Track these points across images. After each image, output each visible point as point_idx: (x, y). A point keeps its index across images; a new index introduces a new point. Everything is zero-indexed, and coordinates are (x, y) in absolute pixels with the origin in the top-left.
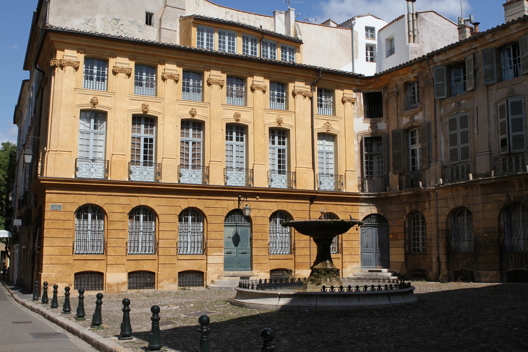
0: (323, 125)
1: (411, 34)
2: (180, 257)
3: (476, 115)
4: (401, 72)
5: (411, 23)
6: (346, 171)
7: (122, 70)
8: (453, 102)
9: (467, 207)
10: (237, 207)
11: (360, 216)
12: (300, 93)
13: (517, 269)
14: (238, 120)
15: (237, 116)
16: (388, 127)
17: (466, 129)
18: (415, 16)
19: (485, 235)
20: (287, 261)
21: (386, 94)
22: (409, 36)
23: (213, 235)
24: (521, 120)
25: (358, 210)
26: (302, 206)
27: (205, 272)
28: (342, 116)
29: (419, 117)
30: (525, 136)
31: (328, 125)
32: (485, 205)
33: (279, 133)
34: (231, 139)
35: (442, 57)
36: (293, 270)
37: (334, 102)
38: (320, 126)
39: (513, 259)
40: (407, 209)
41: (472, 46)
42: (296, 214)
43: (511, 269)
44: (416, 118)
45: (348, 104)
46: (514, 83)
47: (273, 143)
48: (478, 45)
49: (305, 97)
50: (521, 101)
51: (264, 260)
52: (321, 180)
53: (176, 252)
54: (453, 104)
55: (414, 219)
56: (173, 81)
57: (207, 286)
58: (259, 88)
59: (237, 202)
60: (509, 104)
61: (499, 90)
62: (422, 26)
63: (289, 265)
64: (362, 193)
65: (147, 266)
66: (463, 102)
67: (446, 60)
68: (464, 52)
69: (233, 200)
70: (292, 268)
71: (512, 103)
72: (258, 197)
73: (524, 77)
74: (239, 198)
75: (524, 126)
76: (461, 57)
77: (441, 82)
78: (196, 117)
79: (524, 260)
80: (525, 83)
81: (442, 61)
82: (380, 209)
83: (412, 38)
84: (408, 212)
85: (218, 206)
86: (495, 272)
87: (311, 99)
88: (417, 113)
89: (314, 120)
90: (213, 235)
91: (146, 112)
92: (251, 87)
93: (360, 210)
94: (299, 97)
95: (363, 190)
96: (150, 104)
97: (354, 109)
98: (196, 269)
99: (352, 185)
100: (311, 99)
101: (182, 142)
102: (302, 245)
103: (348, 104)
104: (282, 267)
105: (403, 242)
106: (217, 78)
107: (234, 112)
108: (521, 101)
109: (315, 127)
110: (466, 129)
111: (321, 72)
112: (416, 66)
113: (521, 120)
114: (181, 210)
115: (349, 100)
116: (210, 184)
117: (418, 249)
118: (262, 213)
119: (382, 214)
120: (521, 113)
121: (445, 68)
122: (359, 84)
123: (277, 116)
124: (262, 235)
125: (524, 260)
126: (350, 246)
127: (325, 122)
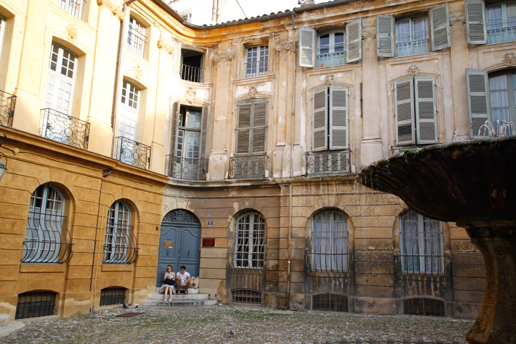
1: (215, 11)
3: (358, 93)
4: (244, 29)
6: (153, 142)
8: (324, 74)
9: (342, 208)
11: (163, 210)
12: (109, 6)
13: (420, 297)
16: (213, 96)
17: (342, 108)
19: (371, 248)
20: (52, 277)
21: (212, 55)
24: (431, 105)
25: (161, 201)
26: (90, 181)
29: (266, 88)
30: (436, 125)
32: (372, 208)
35: (314, 16)
36: (62, 293)
37: (147, 43)
39: (414, 283)
40: (236, 207)
41: (363, 7)
42: (79, 194)
43: (411, 296)
44: (260, 89)
45: (164, 51)
46: (419, 60)
47: (53, 67)
48: (372, 8)
49: (115, 14)
50: (430, 83)
51: (9, 275)
52: (124, 147)
54: (323, 77)
55: (240, 222)
60: (416, 83)
61: (395, 66)
63: (55, 283)
64: (171, 178)
66: (339, 75)
67: (319, 21)
68: (348, 15)
70: (58, 289)
71: (420, 83)
72: (17, 150)
73: (436, 54)
75: (435, 112)
76: (342, 21)
77: (308, 48)
79: (432, 285)
80: (436, 61)
81: (311, 22)
82: (190, 203)
83: (215, 15)
84: (237, 211)
86: (386, 300)
88: (261, 82)
93: (163, 201)
95: (171, 174)
100: (122, 22)
104: (43, 288)
105: (225, 251)
108: (430, 83)
110: (342, 108)
112: (270, 24)
113: (431, 105)
117: (246, 263)
118: (19, 183)
120: (431, 96)
121: (314, 32)
124: (14, 224)
125: (432, 285)
126: (146, 254)
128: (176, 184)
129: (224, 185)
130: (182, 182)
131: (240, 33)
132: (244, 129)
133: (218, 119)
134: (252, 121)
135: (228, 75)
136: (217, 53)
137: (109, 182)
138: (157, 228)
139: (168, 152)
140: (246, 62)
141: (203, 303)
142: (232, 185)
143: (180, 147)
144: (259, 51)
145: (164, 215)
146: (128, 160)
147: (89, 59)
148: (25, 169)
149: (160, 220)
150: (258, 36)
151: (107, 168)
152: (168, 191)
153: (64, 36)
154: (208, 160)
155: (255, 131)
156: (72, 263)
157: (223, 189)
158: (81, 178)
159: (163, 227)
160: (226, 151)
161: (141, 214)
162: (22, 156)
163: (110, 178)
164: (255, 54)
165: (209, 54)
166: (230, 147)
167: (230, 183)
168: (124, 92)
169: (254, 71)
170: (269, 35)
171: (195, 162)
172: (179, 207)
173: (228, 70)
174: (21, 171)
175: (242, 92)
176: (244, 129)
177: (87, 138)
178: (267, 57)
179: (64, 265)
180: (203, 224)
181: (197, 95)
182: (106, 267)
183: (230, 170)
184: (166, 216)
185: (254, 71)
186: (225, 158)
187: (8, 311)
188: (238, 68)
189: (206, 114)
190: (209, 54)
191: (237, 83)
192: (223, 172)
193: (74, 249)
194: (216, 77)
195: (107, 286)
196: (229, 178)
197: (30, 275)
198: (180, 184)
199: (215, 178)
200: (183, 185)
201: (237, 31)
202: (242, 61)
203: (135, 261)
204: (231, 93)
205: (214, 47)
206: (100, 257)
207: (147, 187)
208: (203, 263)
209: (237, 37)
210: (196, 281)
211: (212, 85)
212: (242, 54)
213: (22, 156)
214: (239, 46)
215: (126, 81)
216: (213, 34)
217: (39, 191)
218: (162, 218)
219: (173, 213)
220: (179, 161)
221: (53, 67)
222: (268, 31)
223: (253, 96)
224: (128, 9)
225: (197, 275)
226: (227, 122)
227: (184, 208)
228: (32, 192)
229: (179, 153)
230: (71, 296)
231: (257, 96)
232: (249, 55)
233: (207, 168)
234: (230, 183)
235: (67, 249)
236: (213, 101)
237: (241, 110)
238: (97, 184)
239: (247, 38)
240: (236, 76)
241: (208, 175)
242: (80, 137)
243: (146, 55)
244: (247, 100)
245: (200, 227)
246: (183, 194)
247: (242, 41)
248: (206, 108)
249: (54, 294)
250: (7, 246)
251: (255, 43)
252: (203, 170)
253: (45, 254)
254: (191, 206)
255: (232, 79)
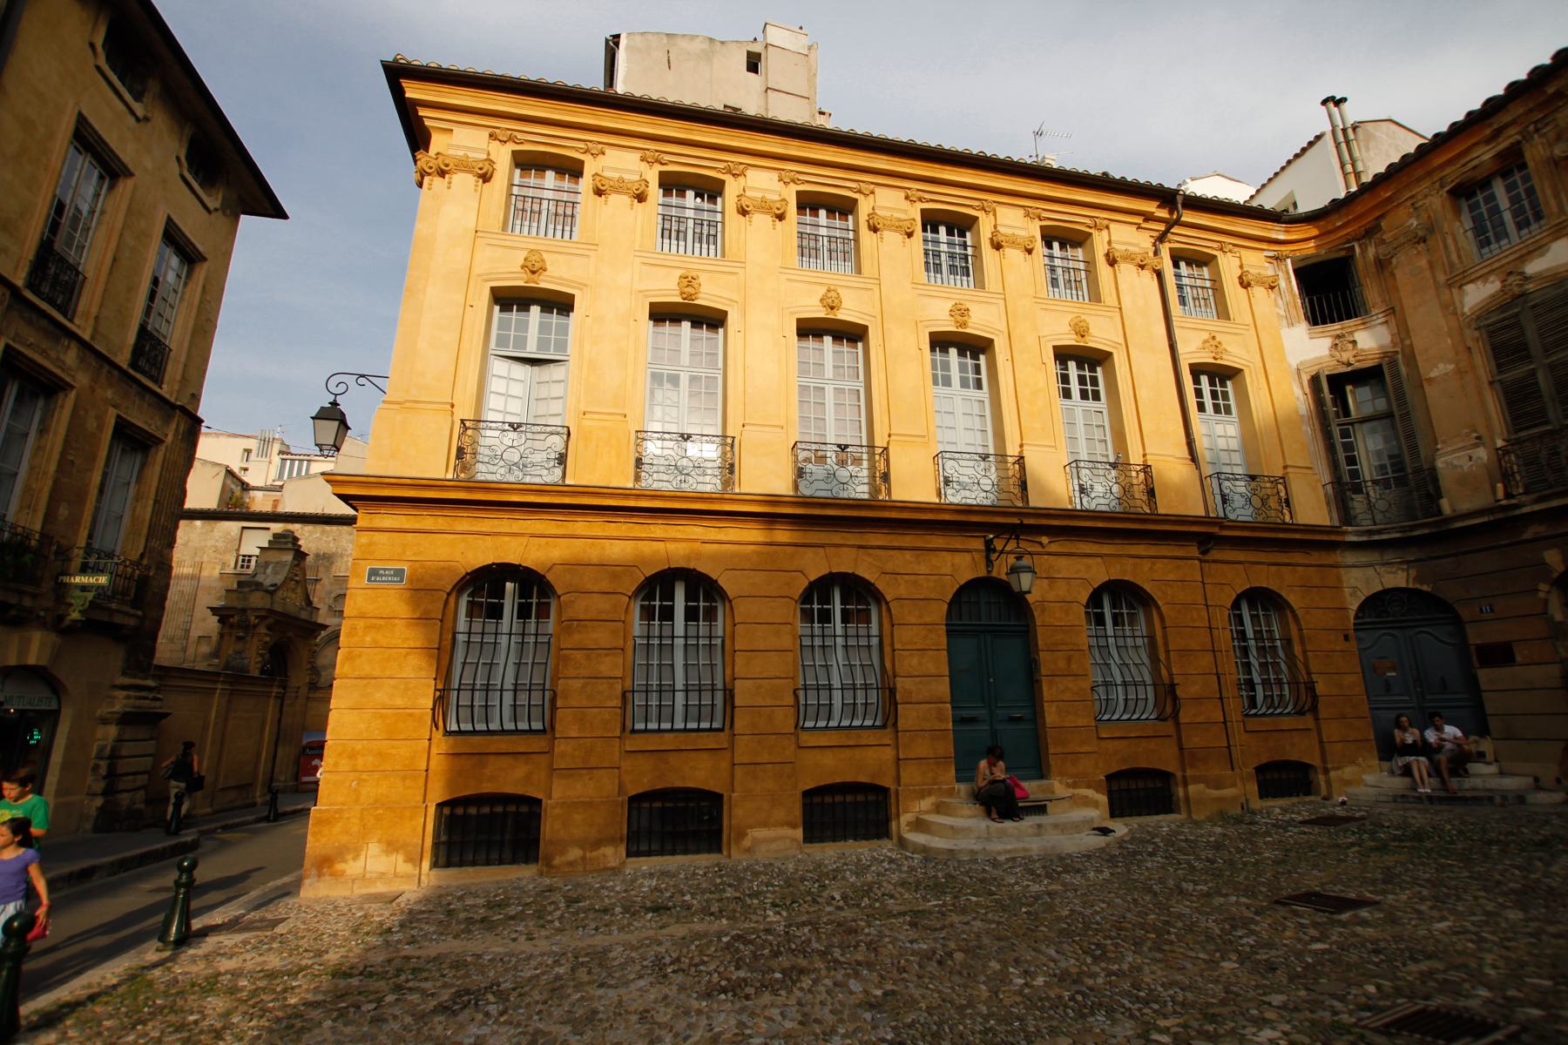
0: (1200, 344)
1: (1349, 168)
2: (807, 739)
4: (1438, 160)
5: (1344, 146)
7: (620, 187)
10: (982, 573)
12: (1129, 258)
14: (964, 324)
15: (961, 312)
16: (1402, 331)
18: (1350, 132)
21: (1371, 251)
22: (1345, 175)
23: (915, 661)
25: (1339, 579)
27: (893, 788)
28: (1249, 320)
31: (1213, 342)
33: (1084, 364)
34: (947, 382)
36: (1179, 774)
38: (1192, 350)
45: (1259, 292)
47: (1067, 394)
49: (1142, 267)
53: (792, 722)
56: (768, 219)
57: (902, 843)
58: (1014, 244)
59: (980, 558)
62: (1372, 153)
63: (1163, 757)
65: (698, 773)
69: (968, 551)
70: (1172, 767)
72: (1045, 540)
74: (988, 543)
78: (842, 315)
82: (1413, 573)
85: (923, 569)
87: (1159, 274)
89: (1178, 333)
90: (915, 661)
91: (690, 296)
92: (992, 240)
93: (1344, 578)
94: (1126, 271)
95: (1347, 517)
96: (703, 278)
97: (1277, 305)
98: (863, 779)
99: (1311, 507)
100: (1159, 274)
101: (803, 389)
102: (1195, 690)
103: (1259, 292)
104: (1143, 764)
106: (896, 215)
107: (949, 305)
109: (1181, 349)
111: (1179, 199)
114: (806, 583)
115: (1261, 283)
116: (894, 498)
118: (1061, 591)
119: (1425, 588)
122: (1282, 237)
123: (1070, 317)
124: (1069, 660)
127: (1206, 336)
128: (1365, 538)
129: (1501, 516)
130: (1379, 532)
131: (1429, 174)
132: (1520, 371)
133: (1433, 375)
134: (1535, 347)
135: (1428, 274)
136: (1383, 242)
137: (1215, 561)
138: (1346, 638)
139: (1326, 477)
140: (1468, 224)
141: (1521, 799)
142: (1525, 510)
143: (1352, 460)
144: (1499, 188)
145: (1355, 607)
146: (1241, 512)
147: (1119, 360)
148: (1064, 566)
149: (1348, 618)
150: (1485, 155)
151: (1204, 536)
152: (1350, 558)
153: (1070, 340)
154: (1433, 469)
155: (1552, 367)
156: (1184, 717)
157: (1499, 526)
158: (1159, 564)
159: (1361, 634)
160: (1478, 438)
161: (1299, 613)
162: (1054, 548)
163: (1215, 554)
164: (1492, 197)
165: (1364, 250)
166: (1489, 427)
167: (1516, 506)
168: (1199, 393)
169: (1501, 234)
170: (1519, 137)
171: (1401, 481)
172: (1389, 585)
173: (1423, 262)
174: (1059, 571)
175: (1476, 295)
176: (1520, 371)
177: (1151, 493)
178: (1531, 192)
179: (1170, 723)
180: (1465, 613)
181: (1359, 346)
182: (1253, 724)
183: (1506, 477)
184: (1361, 608)
185: (1501, 234)
186: (1482, 454)
187: (1096, 804)
188: (1452, 247)
189: (1396, 375)
190: (1364, 250)
191: (1458, 280)
192: (1487, 486)
193: (1179, 692)
194: (1397, 289)
195: (1264, 759)
196: (1508, 495)
197: (1116, 743)
198: (1376, 537)
199: (1465, 506)
200: (1384, 537)
201: (1420, 172)
202: (1460, 230)
203: (1314, 709)
204: (1450, 309)
205: (1371, 232)
206: (1235, 706)
207: (1298, 557)
208: (1492, 704)
209: (1426, 184)
210: (1486, 746)
211: (1391, 311)
212: (1450, 215)
213: (1054, 548)
214: (1437, 202)
215: (1197, 370)
216: (1359, 209)
217: (1095, 599)
218: (1352, 614)
219: (1376, 604)
220: (1358, 489)
221: (1067, 394)
222: (1512, 131)
223: (1517, 290)
224: (1165, 250)
225: (1483, 730)
226: (1460, 372)
227: (1403, 585)
228: (1084, 602)
229: (1355, 474)
230: (1197, 780)
231: (1530, 287)
232: (1472, 208)
233: (1438, 488)
234: (1516, 506)
235: (1168, 694)
236: (1407, 342)
237: (1491, 334)
238: (1192, 570)
239: (1453, 174)
240: (1452, 265)
241: (1445, 505)
242: (1139, 492)
243: (1223, 313)
244: (1502, 308)
245: (1457, 621)
246: (1389, 556)
247: (1442, 187)
248: (1393, 363)
249: (1166, 776)
250: (1067, 696)
251: (1480, 174)
252: (1429, 495)
253: (1131, 704)
254: (1417, 579)
255: (1442, 278)
